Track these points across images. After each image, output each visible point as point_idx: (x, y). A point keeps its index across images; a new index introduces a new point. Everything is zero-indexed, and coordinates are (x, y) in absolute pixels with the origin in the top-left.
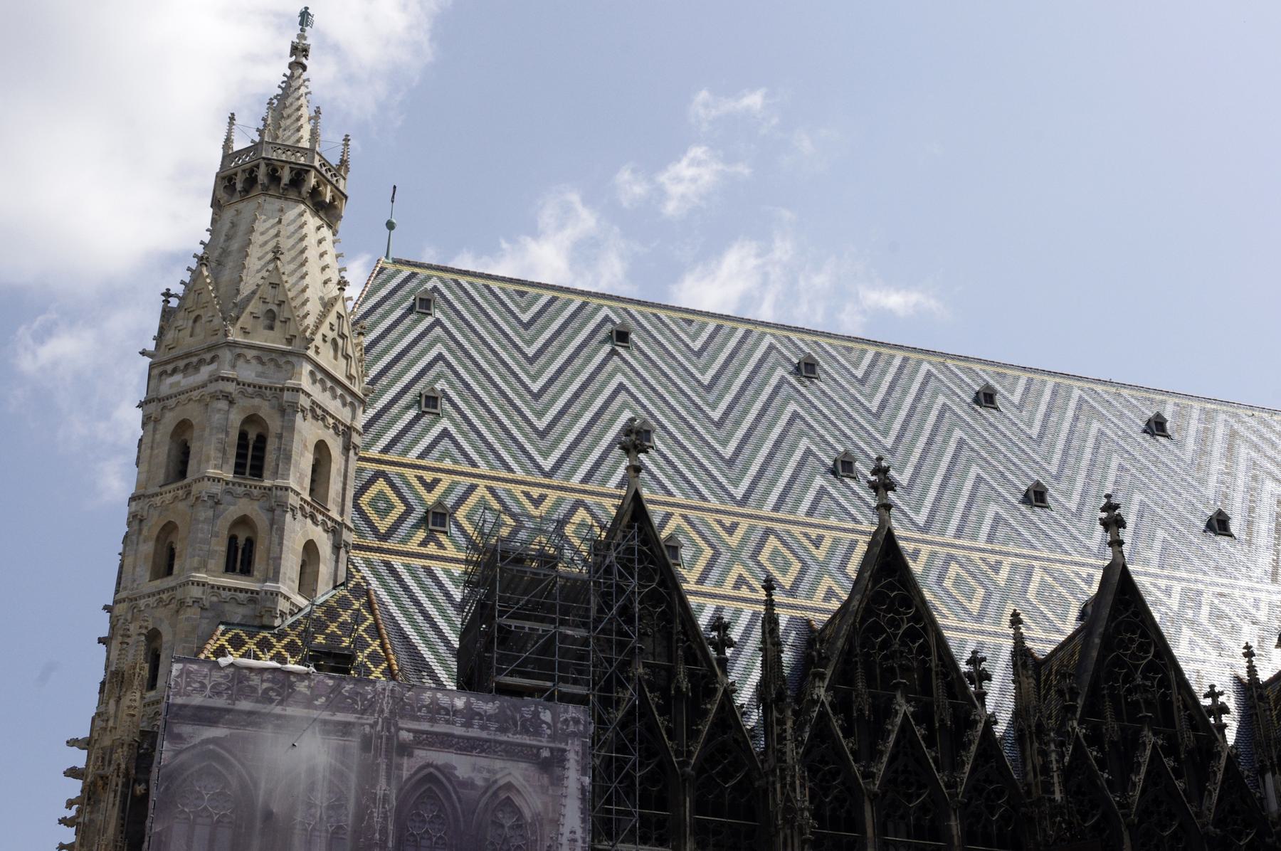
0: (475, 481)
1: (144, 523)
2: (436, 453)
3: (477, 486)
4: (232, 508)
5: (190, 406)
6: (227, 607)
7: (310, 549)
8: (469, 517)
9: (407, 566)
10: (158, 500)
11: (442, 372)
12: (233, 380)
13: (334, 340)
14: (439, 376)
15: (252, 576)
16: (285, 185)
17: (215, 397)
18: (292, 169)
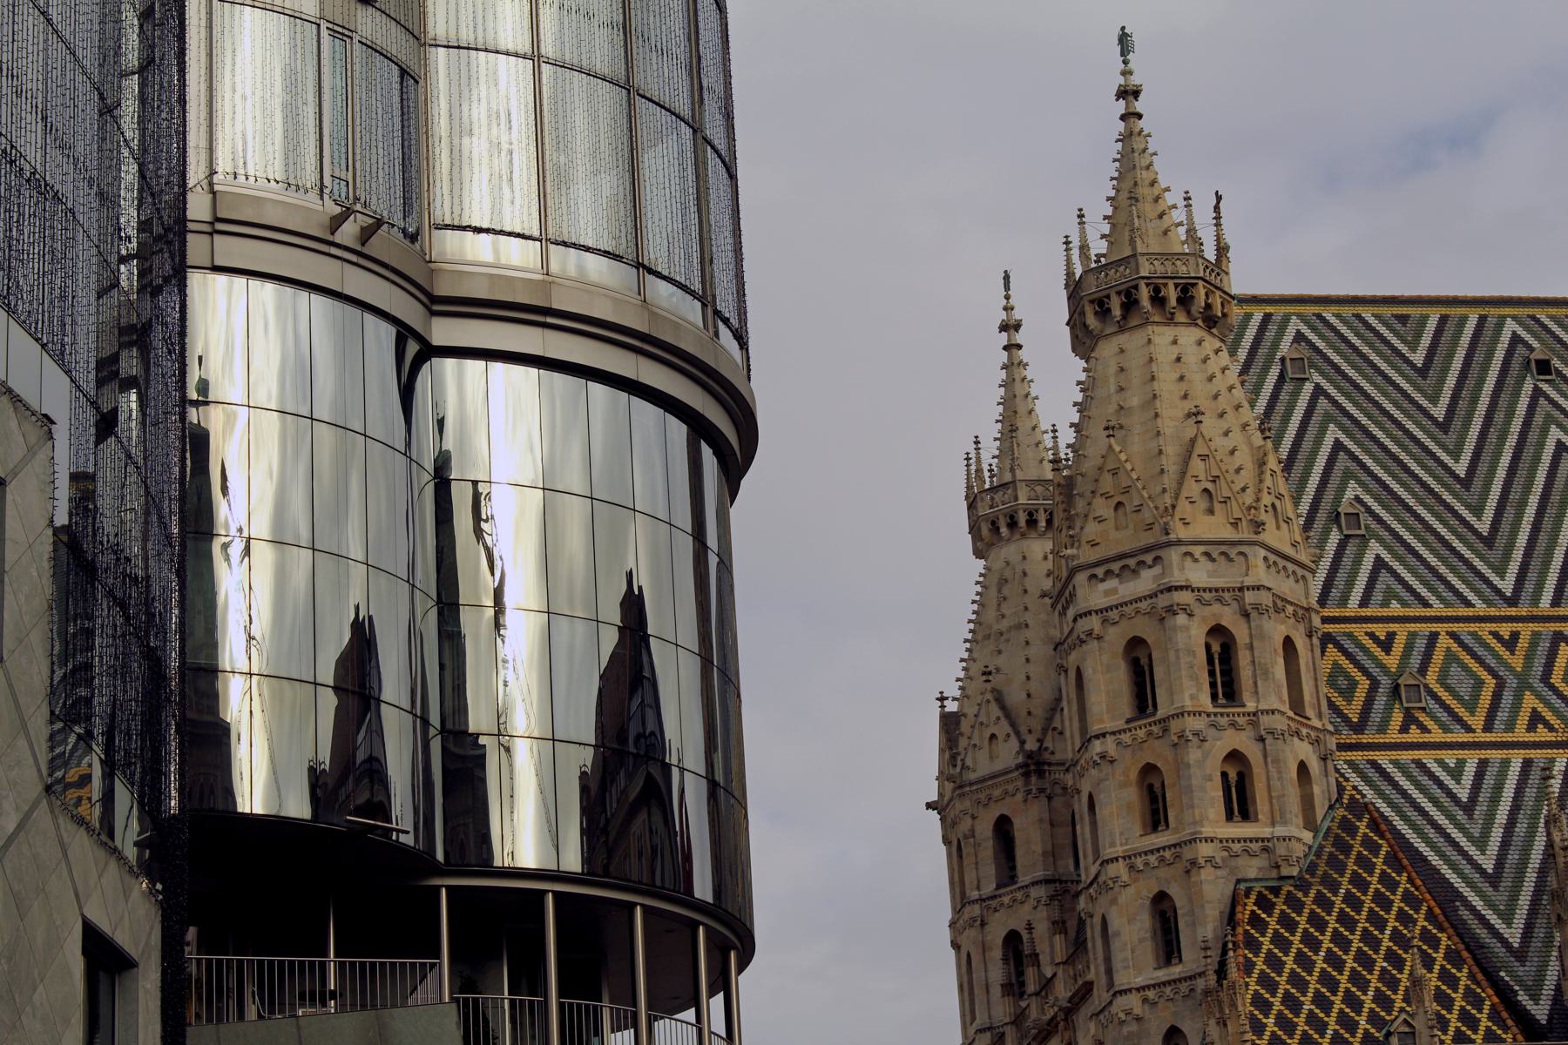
0: (1435, 627)
1: (1116, 763)
2: (1378, 596)
3: (1437, 634)
4: (1218, 743)
5: (1139, 620)
6: (1240, 862)
7: (1303, 768)
8: (1443, 680)
9: (1395, 763)
10: (1126, 738)
11: (1347, 468)
12: (1186, 587)
13: (1273, 505)
14: (1347, 476)
15: (1257, 820)
16: (1174, 308)
17: (1171, 610)
18: (1176, 286)
